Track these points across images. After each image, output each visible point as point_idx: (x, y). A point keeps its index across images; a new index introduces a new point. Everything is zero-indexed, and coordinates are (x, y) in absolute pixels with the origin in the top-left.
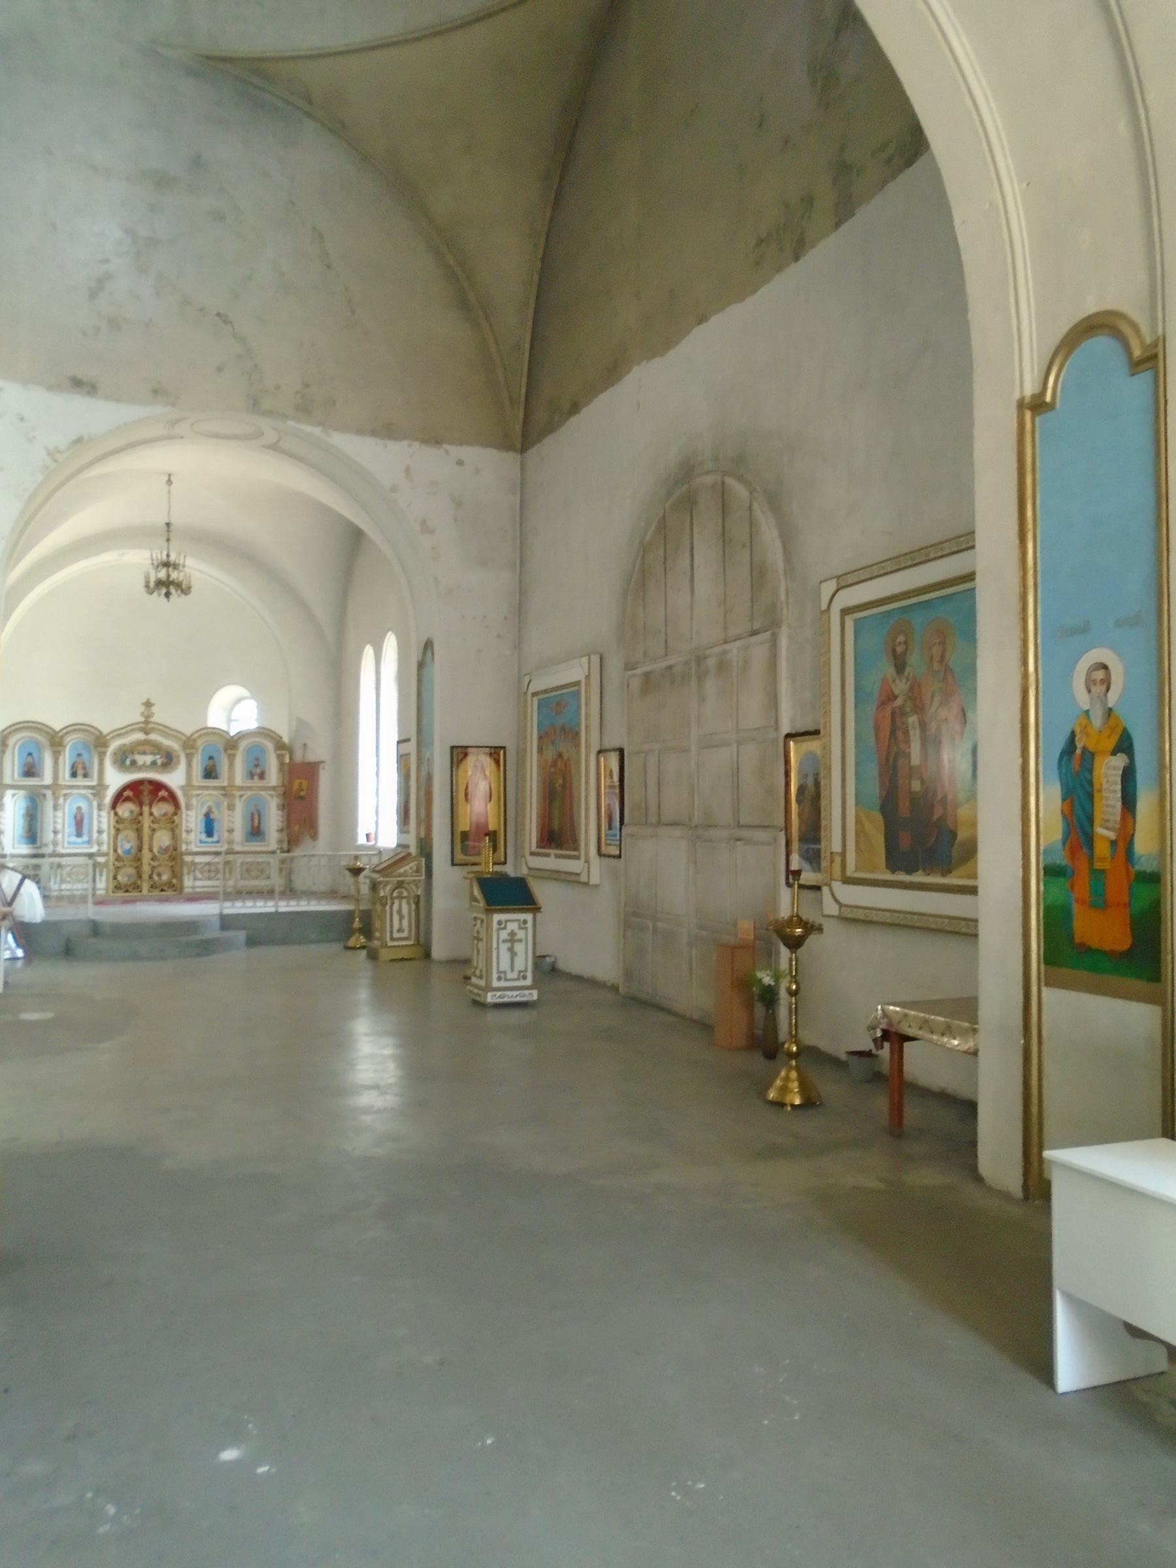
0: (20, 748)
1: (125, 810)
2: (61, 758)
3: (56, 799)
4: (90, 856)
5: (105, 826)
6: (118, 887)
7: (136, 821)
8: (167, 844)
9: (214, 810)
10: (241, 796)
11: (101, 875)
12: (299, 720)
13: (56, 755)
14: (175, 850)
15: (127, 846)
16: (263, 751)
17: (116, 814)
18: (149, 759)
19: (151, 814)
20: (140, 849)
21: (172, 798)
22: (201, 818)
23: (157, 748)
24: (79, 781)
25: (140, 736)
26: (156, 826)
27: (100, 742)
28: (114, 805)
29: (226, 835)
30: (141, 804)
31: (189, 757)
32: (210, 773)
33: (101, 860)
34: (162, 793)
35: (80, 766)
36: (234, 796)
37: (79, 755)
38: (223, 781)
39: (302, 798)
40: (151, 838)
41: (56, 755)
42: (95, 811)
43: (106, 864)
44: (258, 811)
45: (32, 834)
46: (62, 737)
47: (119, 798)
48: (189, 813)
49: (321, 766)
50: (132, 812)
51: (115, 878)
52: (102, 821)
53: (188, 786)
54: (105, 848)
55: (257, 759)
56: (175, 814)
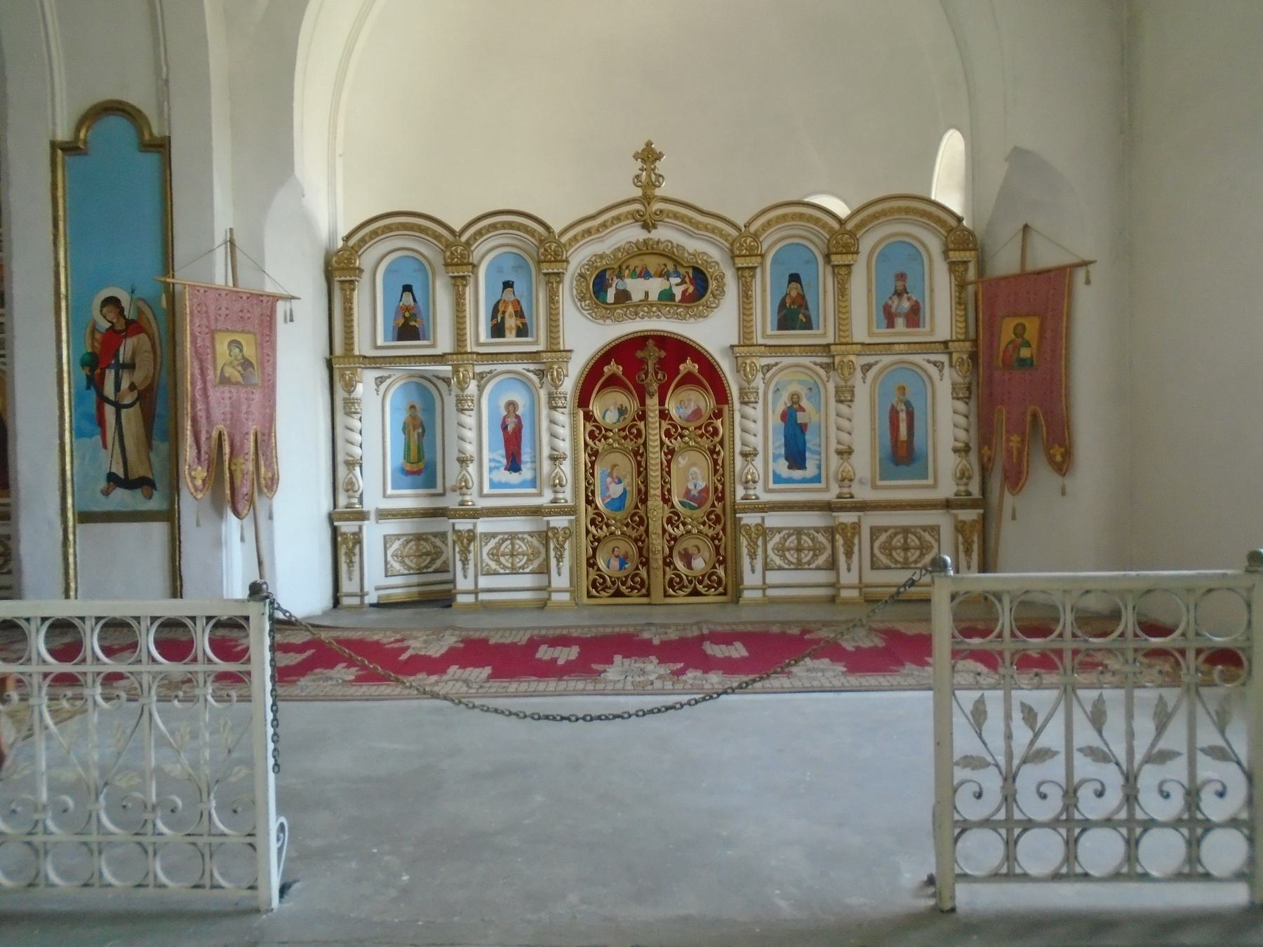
0: (388, 271)
1: (608, 407)
2: (469, 292)
3: (462, 385)
4: (536, 511)
5: (564, 446)
6: (598, 585)
7: (633, 432)
8: (702, 484)
9: (804, 403)
10: (866, 368)
11: (559, 559)
12: (1019, 156)
13: (459, 283)
14: (721, 499)
15: (616, 490)
16: (915, 252)
17: (588, 417)
18: (655, 286)
19: (664, 415)
20: (643, 498)
21: (710, 377)
22: (775, 421)
23: (671, 260)
24: (511, 343)
25: (634, 234)
26: (676, 444)
27: (545, 250)
28: (583, 400)
29: (834, 460)
30: (642, 394)
31: (745, 275)
32: (793, 314)
33: (560, 522)
34: (689, 366)
35: (510, 309)
36: (851, 365)
37: (508, 285)
38: (824, 333)
39: (1022, 362)
40: (666, 471)
42: (544, 411)
43: (569, 533)
44: (908, 404)
45: (420, 465)
46: (468, 244)
47: (592, 381)
48: (748, 410)
49: (1080, 275)
50: (622, 411)
51: (591, 564)
52: (559, 432)
53: (744, 345)
54: (566, 495)
55: (901, 277)
56: (718, 415)
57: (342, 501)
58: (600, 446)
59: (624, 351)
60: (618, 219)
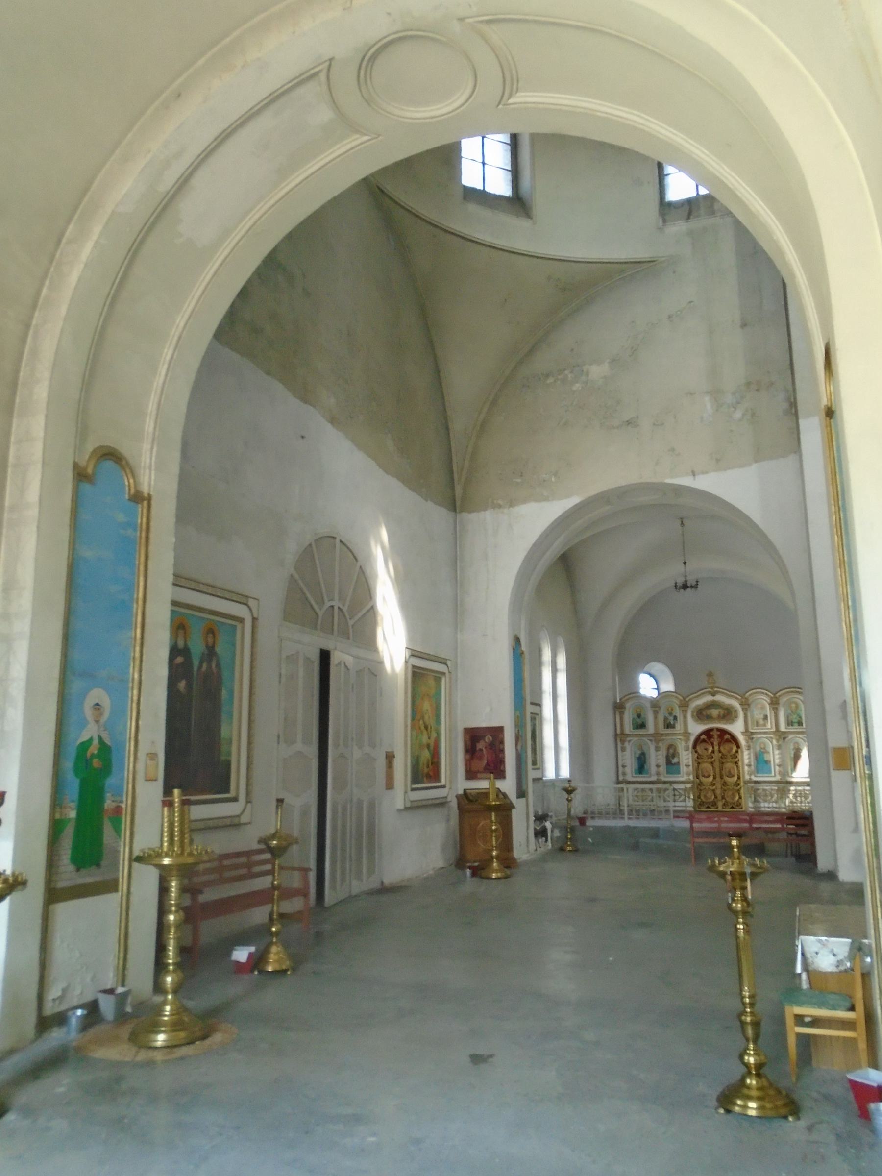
19: (720, 751)
28: (695, 746)
34: (727, 737)
41: (656, 713)
51: (699, 797)
52: (686, 757)
57: (621, 778)
58: (700, 761)
59: (708, 733)
60: (703, 694)
